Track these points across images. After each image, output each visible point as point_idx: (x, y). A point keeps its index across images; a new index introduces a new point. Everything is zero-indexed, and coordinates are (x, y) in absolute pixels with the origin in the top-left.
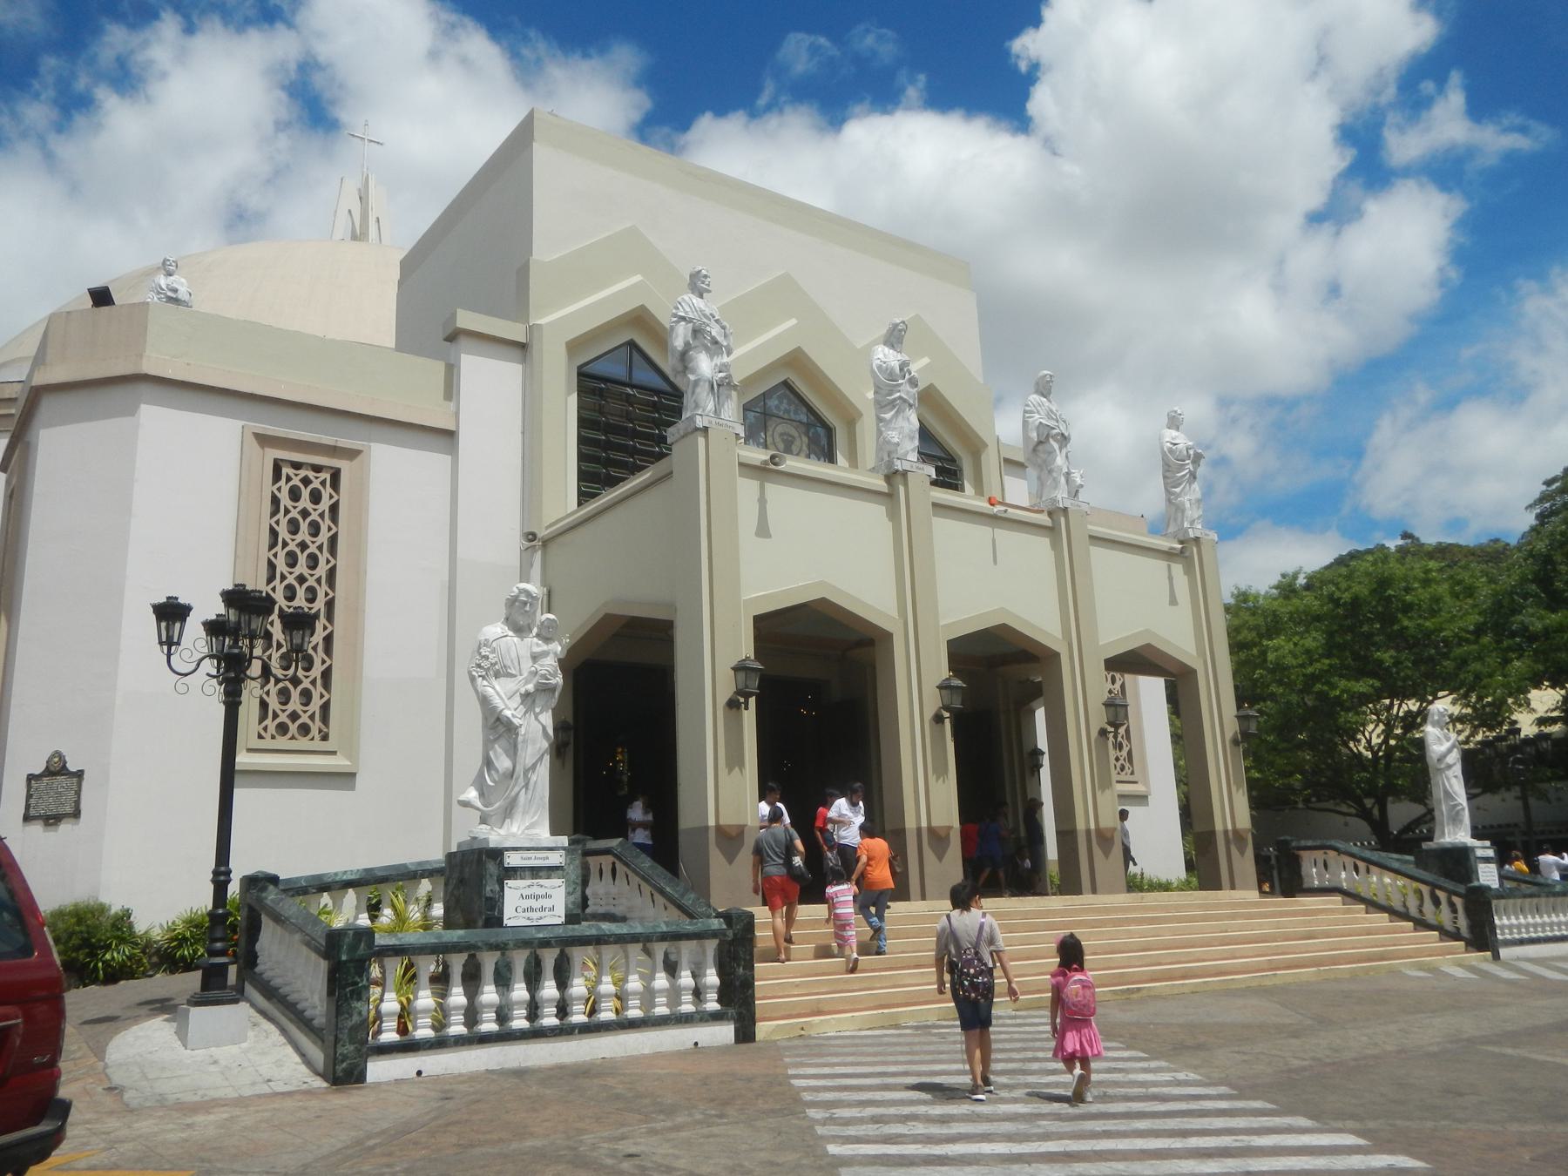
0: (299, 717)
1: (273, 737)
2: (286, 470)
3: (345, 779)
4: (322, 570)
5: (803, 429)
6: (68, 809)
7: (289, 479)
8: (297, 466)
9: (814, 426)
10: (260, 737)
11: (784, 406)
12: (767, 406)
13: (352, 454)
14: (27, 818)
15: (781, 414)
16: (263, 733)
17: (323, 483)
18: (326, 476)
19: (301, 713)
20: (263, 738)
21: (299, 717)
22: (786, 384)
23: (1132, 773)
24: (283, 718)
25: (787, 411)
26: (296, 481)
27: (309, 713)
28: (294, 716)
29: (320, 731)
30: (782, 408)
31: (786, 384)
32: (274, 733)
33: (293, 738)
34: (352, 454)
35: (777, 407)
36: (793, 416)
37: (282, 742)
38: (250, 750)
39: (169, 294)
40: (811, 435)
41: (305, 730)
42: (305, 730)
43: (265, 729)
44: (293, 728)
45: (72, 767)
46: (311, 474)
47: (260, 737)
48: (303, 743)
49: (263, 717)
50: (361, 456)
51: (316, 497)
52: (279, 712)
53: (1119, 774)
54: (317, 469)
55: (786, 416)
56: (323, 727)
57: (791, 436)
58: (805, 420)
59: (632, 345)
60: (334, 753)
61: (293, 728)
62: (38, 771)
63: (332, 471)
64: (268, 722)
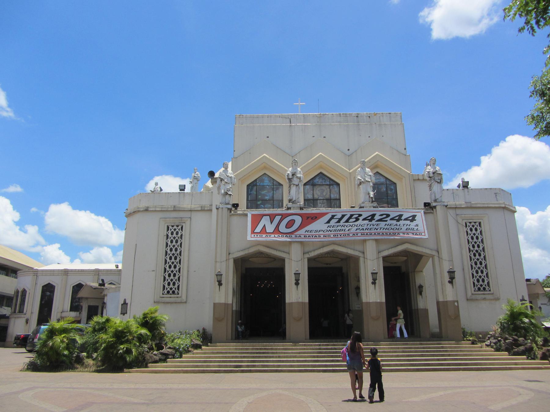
0: (172, 289)
1: (166, 294)
2: (170, 227)
4: (178, 252)
5: (327, 187)
6: (125, 312)
9: (332, 185)
10: (163, 294)
11: (321, 180)
12: (314, 182)
14: (121, 314)
15: (319, 183)
16: (164, 293)
17: (179, 230)
18: (180, 227)
19: (173, 288)
21: (172, 289)
22: (321, 173)
23: (490, 291)
24: (169, 289)
25: (321, 182)
26: (172, 230)
27: (175, 288)
28: (171, 289)
29: (177, 292)
30: (320, 181)
31: (321, 173)
32: (166, 293)
33: (171, 294)
35: (317, 182)
36: (324, 183)
38: (160, 297)
39: (195, 178)
40: (331, 188)
41: (174, 292)
42: (174, 292)
43: (164, 292)
44: (171, 292)
45: (127, 302)
46: (175, 227)
47: (163, 294)
48: (173, 296)
49: (164, 289)
52: (168, 288)
53: (482, 291)
55: (321, 184)
56: (178, 291)
57: (322, 190)
58: (328, 183)
59: (265, 174)
61: (171, 292)
62: (123, 303)
63: (181, 226)
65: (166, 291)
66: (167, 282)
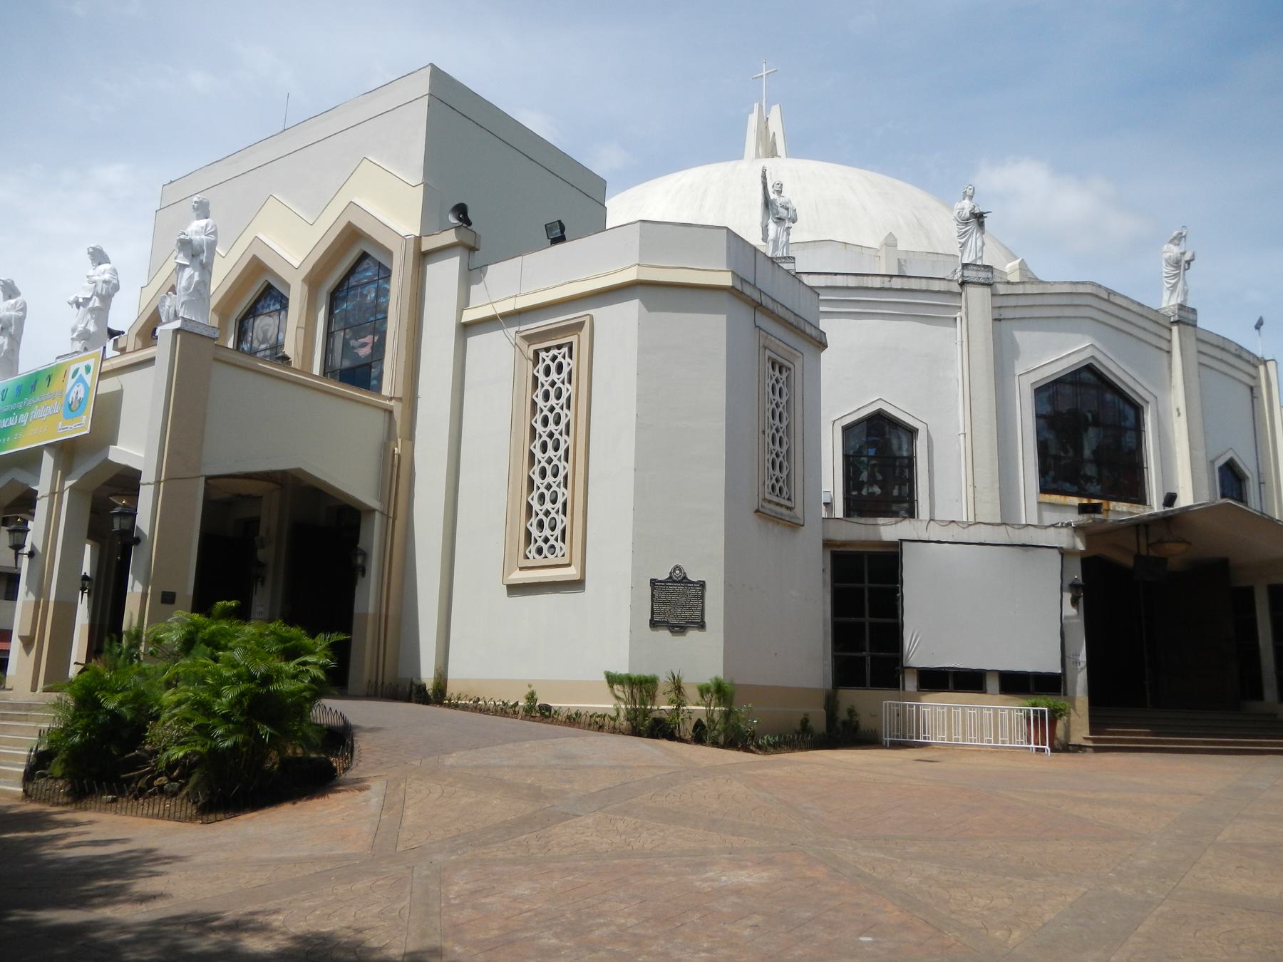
2: (543, 354)
3: (577, 585)
7: (544, 360)
8: (547, 350)
13: (580, 326)
18: (565, 350)
20: (528, 558)
24: (540, 543)
33: (546, 557)
34: (578, 327)
37: (539, 560)
38: (521, 569)
46: (555, 352)
48: (552, 560)
50: (587, 326)
51: (560, 368)
54: (559, 347)
60: (569, 565)
63: (568, 345)
64: (533, 547)
65: (533, 547)
66: (536, 520)
